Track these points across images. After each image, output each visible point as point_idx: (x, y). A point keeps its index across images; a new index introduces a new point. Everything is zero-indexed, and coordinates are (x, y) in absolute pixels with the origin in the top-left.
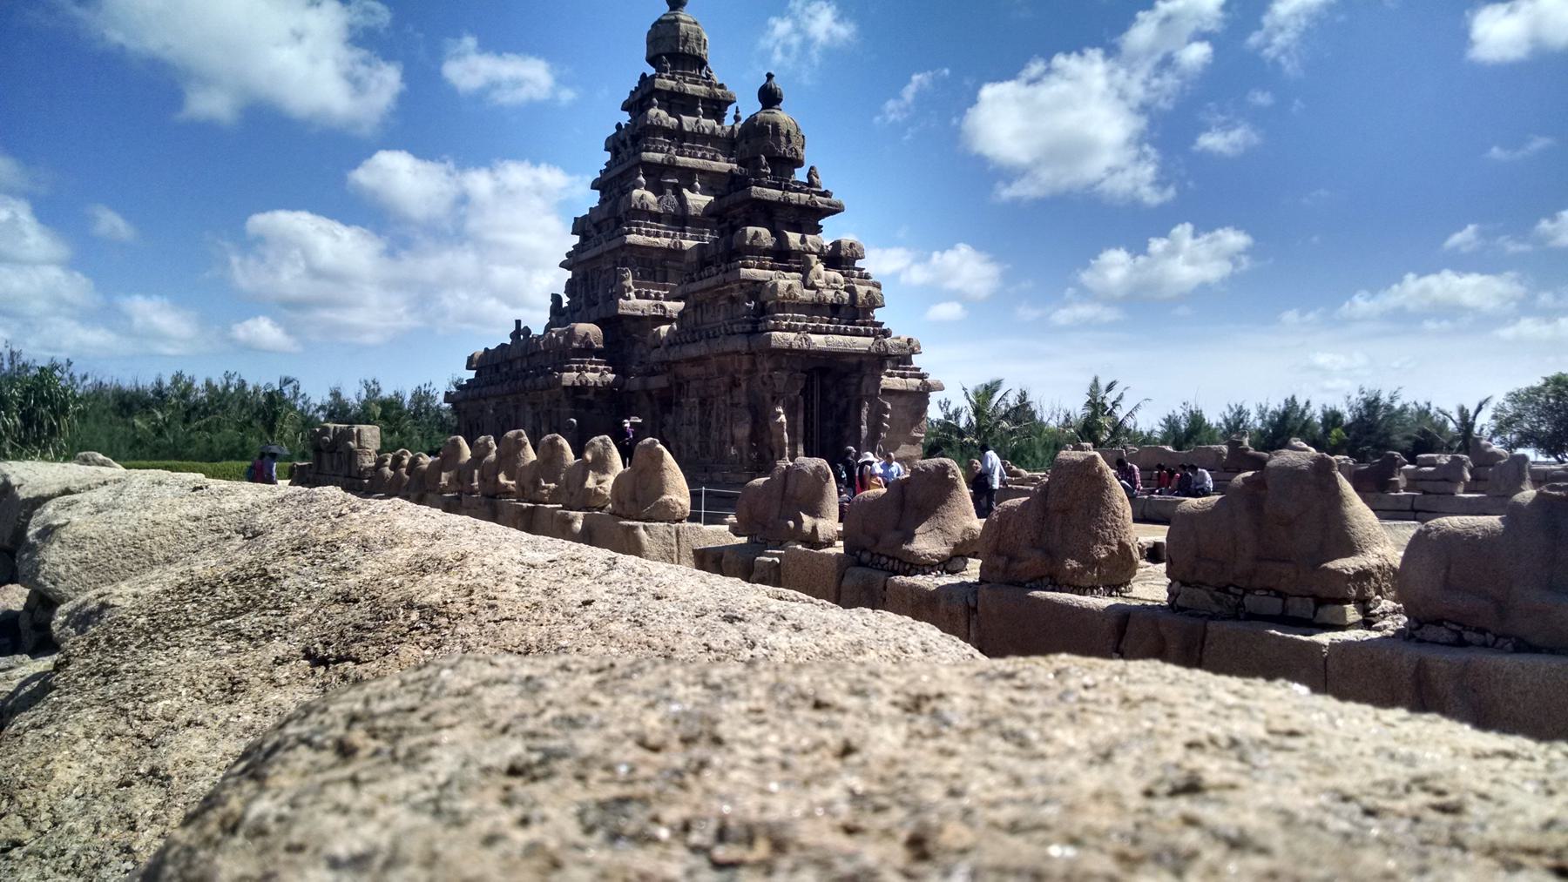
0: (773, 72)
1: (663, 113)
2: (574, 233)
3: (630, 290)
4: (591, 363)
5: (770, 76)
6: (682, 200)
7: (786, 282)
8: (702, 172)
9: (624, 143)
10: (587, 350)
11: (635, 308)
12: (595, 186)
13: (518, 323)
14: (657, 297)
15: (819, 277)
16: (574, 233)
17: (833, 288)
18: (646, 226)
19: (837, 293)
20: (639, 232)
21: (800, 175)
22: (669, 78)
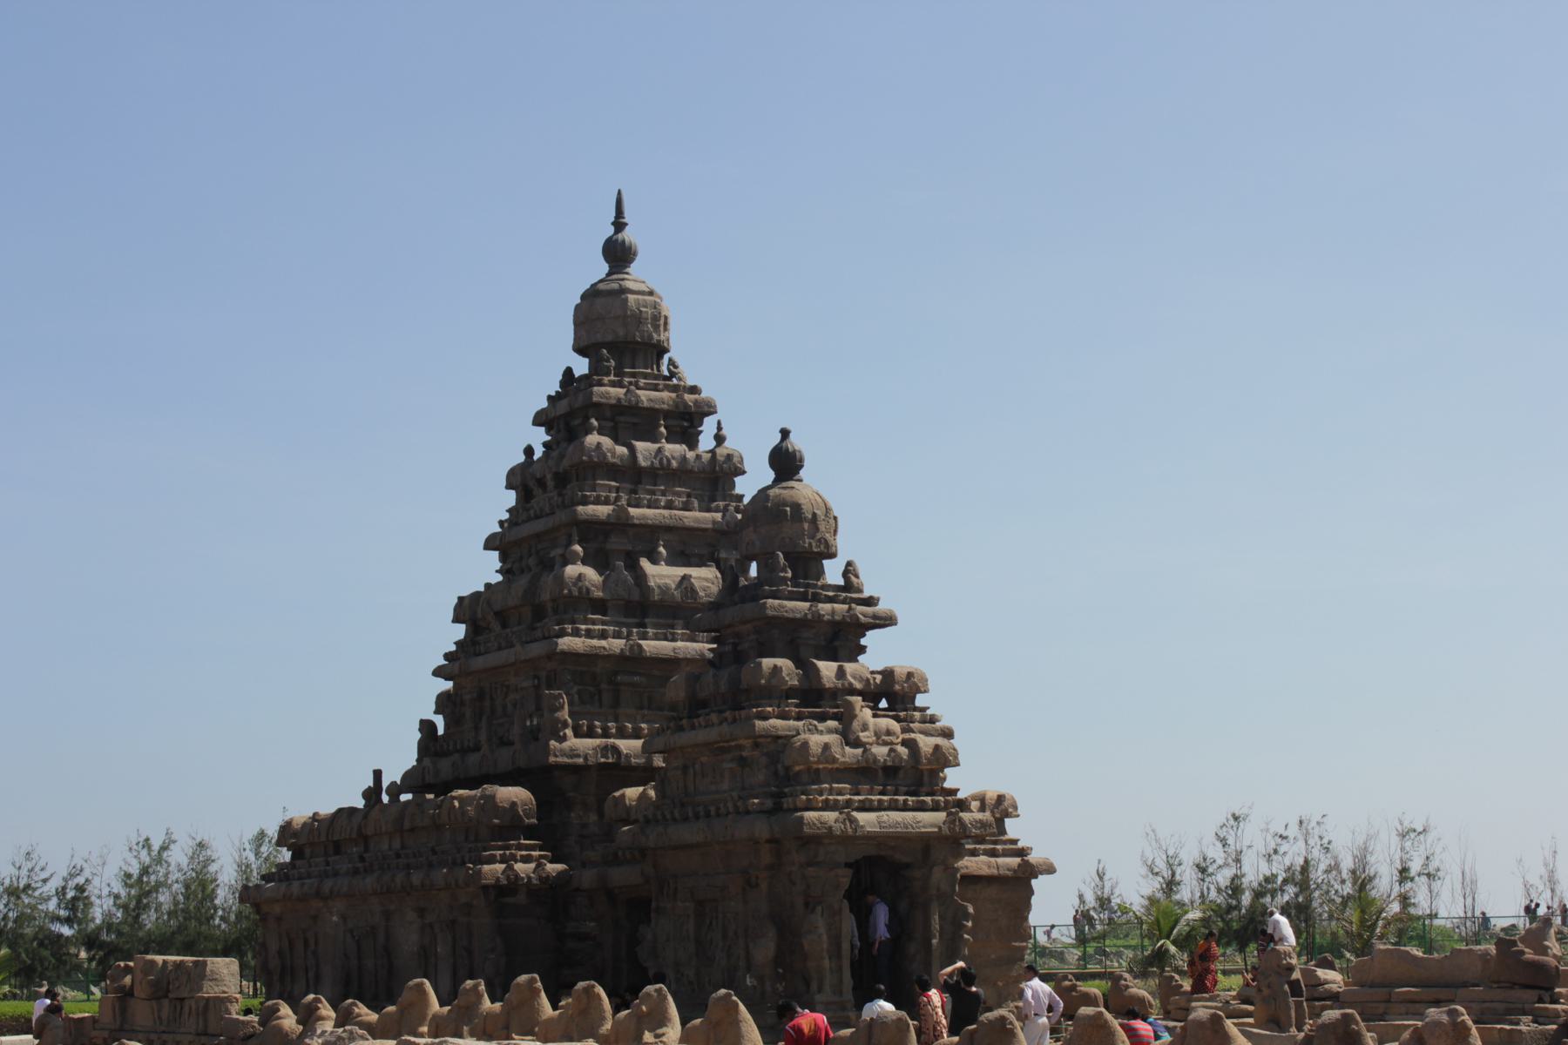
0: (788, 427)
1: (606, 442)
2: (457, 619)
3: (565, 725)
4: (520, 847)
5: (785, 433)
6: (641, 577)
7: (820, 737)
8: (668, 529)
9: (541, 483)
10: (509, 827)
11: (573, 753)
12: (490, 544)
13: (378, 774)
14: (606, 734)
15: (865, 728)
16: (457, 619)
17: (885, 743)
18: (586, 622)
19: (891, 750)
20: (576, 633)
21: (833, 573)
22: (613, 384)
